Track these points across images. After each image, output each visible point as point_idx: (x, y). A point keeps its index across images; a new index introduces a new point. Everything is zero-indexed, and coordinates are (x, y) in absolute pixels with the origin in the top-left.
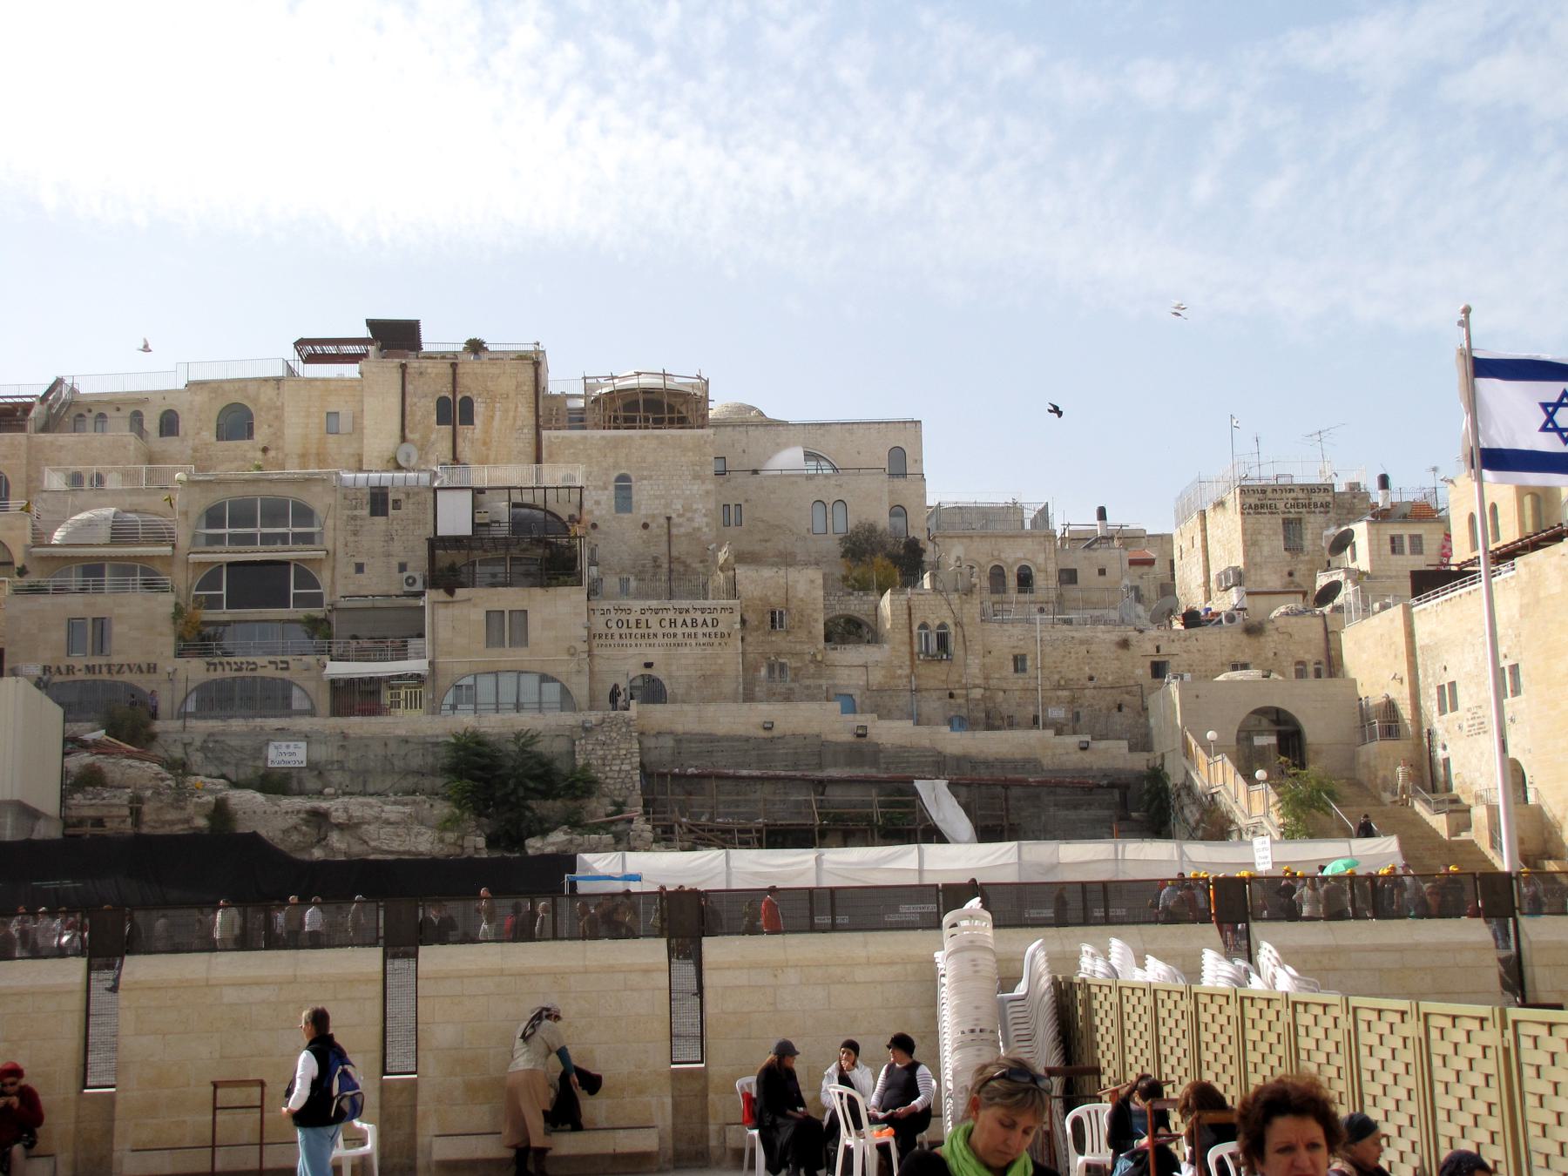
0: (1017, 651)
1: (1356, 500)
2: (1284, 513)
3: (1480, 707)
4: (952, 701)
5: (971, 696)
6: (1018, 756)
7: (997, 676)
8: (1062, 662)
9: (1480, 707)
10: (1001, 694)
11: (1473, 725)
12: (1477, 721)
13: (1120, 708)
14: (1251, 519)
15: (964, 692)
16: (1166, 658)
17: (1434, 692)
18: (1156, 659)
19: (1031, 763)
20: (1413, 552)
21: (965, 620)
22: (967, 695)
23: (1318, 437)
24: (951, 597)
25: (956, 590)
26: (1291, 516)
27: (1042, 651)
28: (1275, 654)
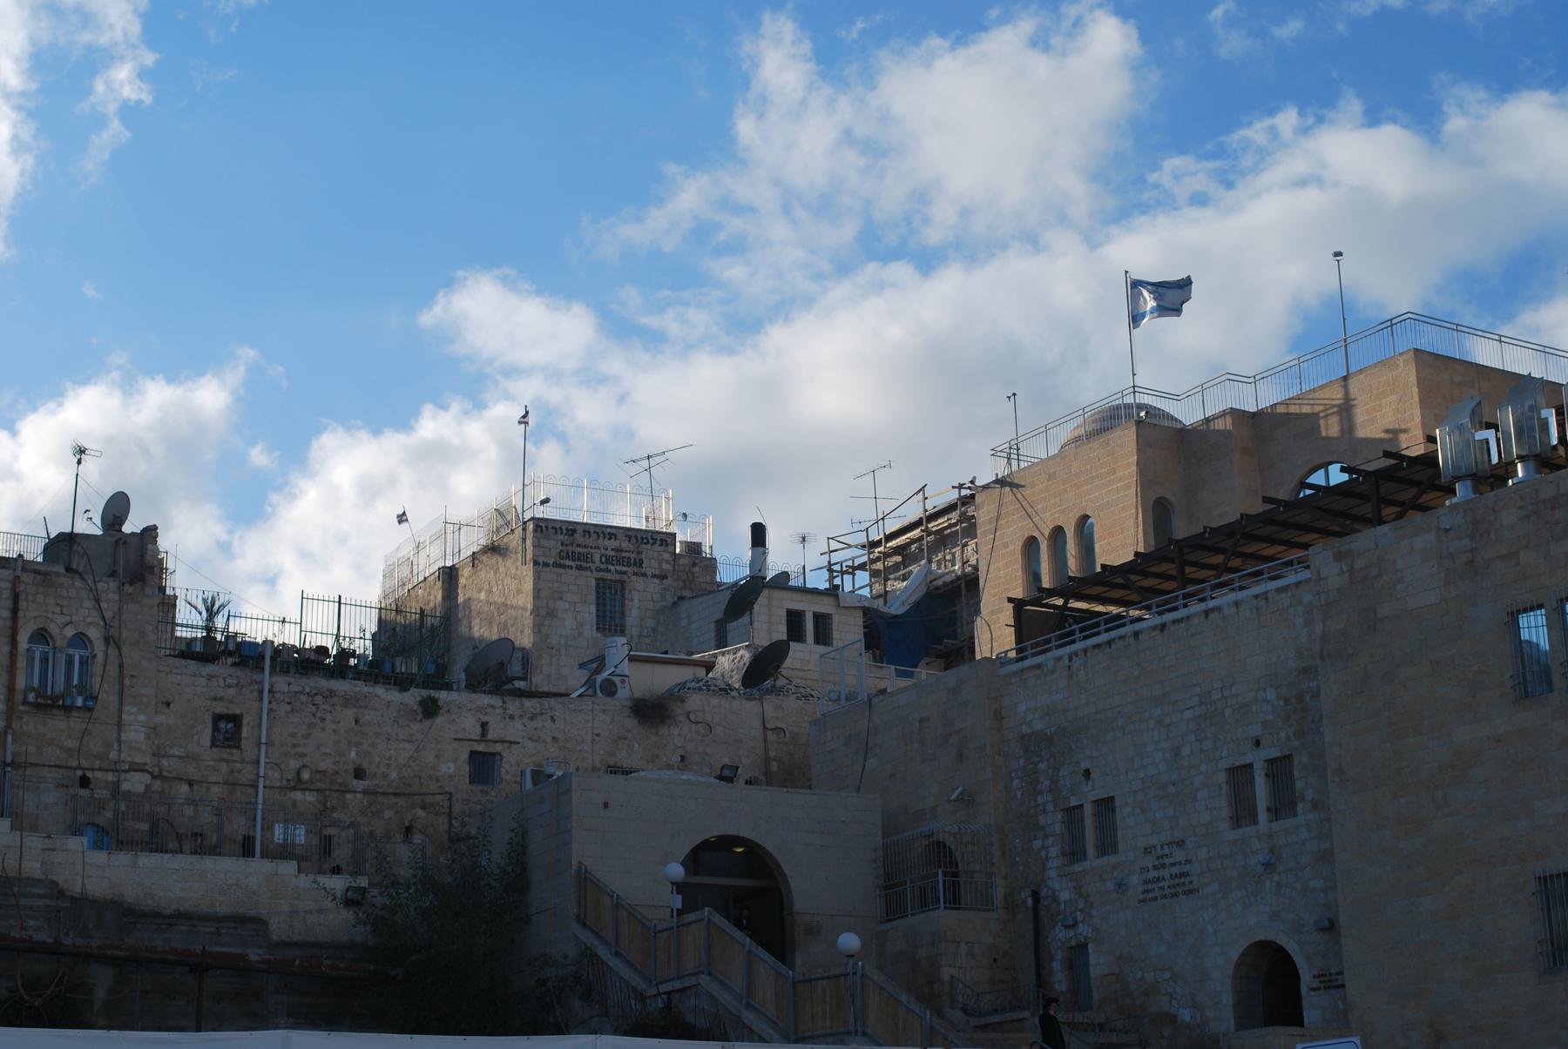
0: (220, 708)
1: (696, 569)
2: (600, 570)
3: (1181, 844)
4: (84, 792)
5: (125, 786)
6: (222, 909)
7: (176, 752)
8: (307, 736)
9: (1181, 844)
10: (185, 788)
11: (1159, 880)
12: (1165, 873)
13: (408, 831)
14: (549, 574)
15: (110, 777)
16: (498, 748)
17: (1054, 821)
18: (481, 748)
19: (250, 923)
20: (817, 641)
21: (125, 634)
22: (117, 783)
23: (645, 464)
24: (101, 586)
25: (113, 574)
26: (609, 576)
27: (270, 711)
28: (683, 758)
